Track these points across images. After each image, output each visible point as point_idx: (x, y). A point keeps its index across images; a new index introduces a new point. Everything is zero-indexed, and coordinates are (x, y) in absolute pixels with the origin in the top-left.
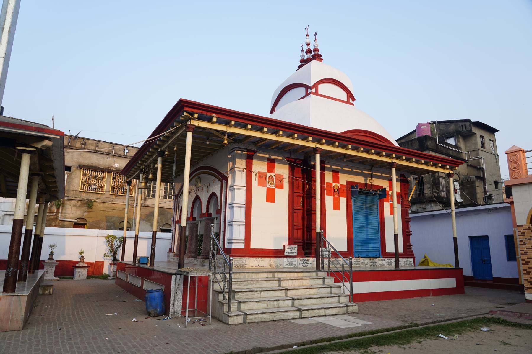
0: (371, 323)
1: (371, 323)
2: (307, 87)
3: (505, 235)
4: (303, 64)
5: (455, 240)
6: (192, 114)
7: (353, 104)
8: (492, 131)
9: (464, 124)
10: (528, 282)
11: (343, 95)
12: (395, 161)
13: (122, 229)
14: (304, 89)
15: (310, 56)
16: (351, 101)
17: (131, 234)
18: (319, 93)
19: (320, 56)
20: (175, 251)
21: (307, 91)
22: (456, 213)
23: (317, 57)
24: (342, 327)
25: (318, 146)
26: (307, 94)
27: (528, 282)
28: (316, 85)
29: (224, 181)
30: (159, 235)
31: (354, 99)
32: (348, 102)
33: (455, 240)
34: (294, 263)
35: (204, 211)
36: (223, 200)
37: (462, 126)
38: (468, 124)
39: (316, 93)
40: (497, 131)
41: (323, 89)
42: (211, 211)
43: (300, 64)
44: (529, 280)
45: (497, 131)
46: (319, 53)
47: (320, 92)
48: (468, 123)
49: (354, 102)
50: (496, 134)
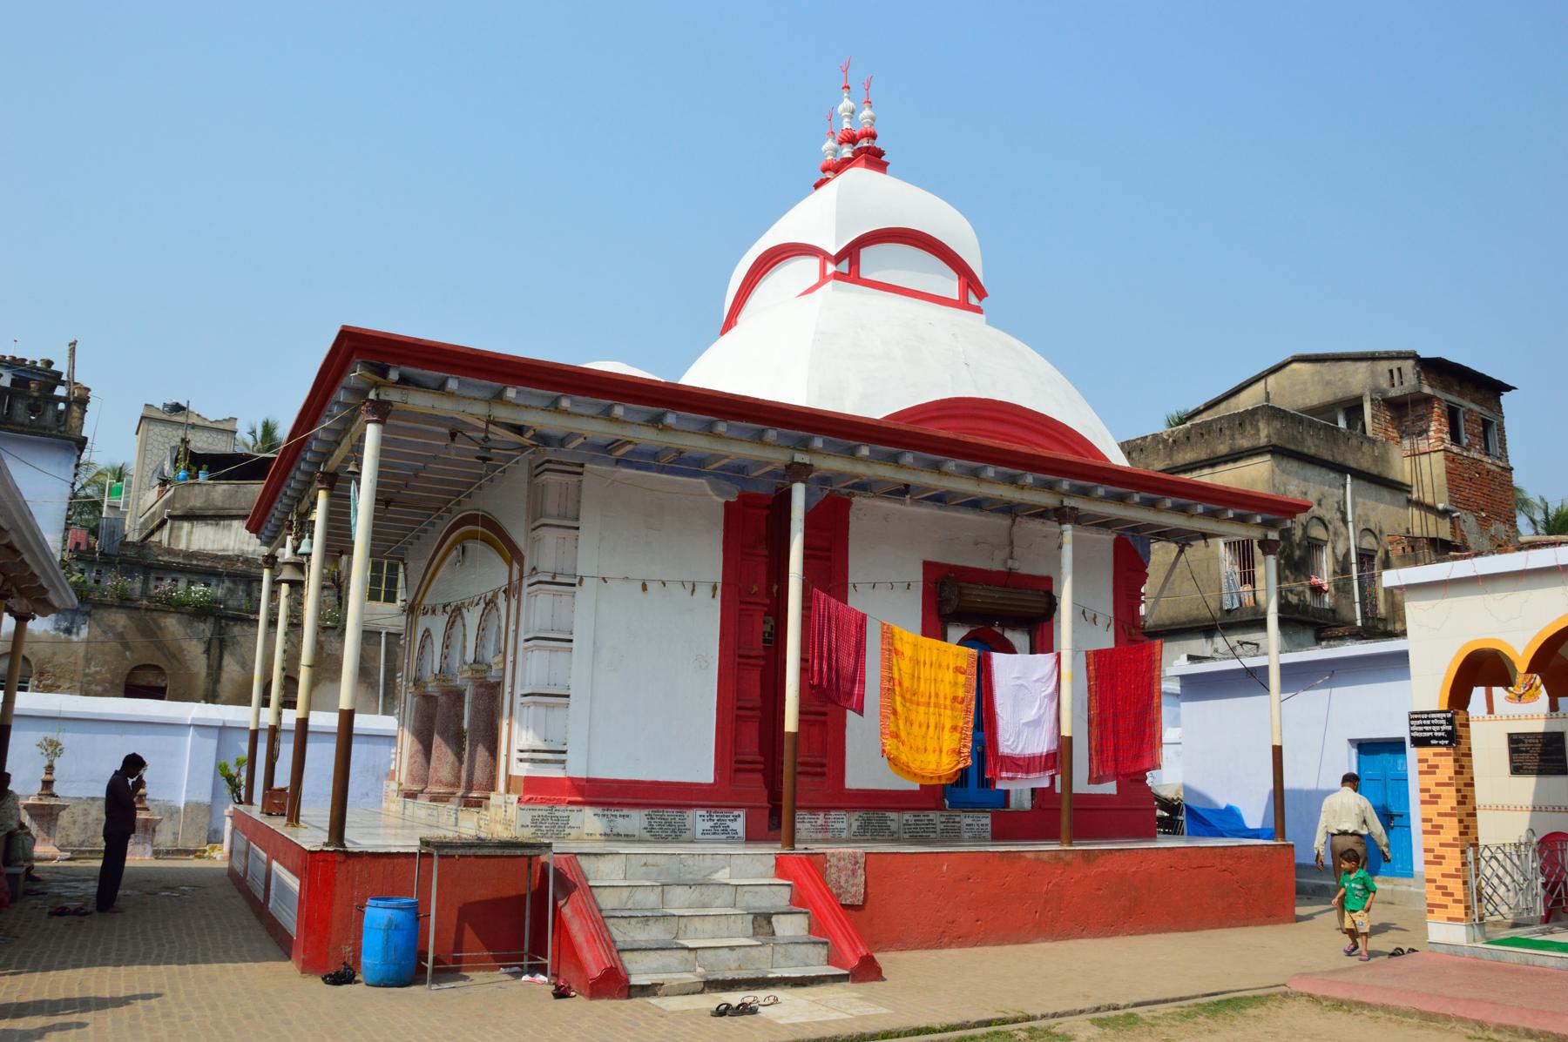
0: (885, 1011)
1: (885, 1011)
4: (829, 175)
5: (1277, 752)
6: (383, 373)
7: (978, 310)
8: (1491, 389)
9: (1395, 364)
10: (1438, 888)
12: (1068, 502)
13: (248, 703)
14: (813, 263)
15: (847, 151)
16: (973, 300)
17: (290, 718)
18: (863, 275)
19: (882, 153)
20: (403, 779)
22: (1285, 668)
24: (780, 1022)
25: (800, 458)
26: (824, 279)
27: (1438, 888)
28: (851, 252)
29: (516, 567)
30: (362, 722)
31: (981, 294)
32: (962, 304)
33: (1277, 752)
34: (732, 825)
35: (470, 657)
36: (512, 627)
37: (1391, 371)
38: (1408, 365)
39: (853, 276)
40: (1509, 388)
41: (874, 262)
42: (490, 655)
44: (1442, 882)
45: (1509, 388)
46: (878, 144)
47: (865, 274)
48: (1411, 363)
49: (983, 304)
50: (1505, 398)
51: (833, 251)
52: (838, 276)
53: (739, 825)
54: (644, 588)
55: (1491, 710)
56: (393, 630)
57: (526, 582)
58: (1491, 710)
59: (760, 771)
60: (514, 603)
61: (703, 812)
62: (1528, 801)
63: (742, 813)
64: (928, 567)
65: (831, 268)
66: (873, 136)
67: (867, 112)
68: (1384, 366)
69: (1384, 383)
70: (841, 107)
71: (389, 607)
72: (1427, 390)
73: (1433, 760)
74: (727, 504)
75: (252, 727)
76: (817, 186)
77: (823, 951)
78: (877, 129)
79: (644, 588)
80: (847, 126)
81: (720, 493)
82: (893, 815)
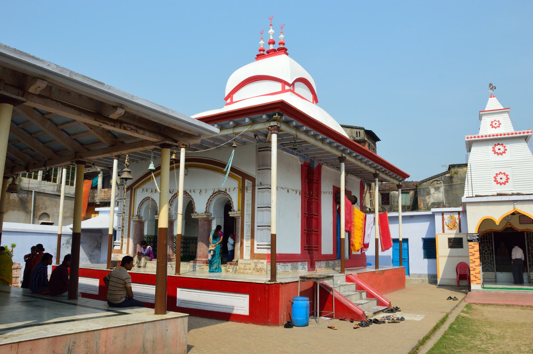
2: (284, 83)
3: (422, 238)
9: (358, 131)
11: (310, 96)
15: (272, 47)
19: (286, 50)
21: (283, 88)
23: (283, 50)
28: (293, 84)
38: (362, 132)
39: (293, 91)
40: (379, 140)
43: (259, 53)
45: (379, 140)
46: (285, 46)
47: (296, 90)
51: (291, 83)
52: (290, 90)
53: (306, 267)
54: (288, 191)
55: (444, 232)
56: (37, 190)
57: (257, 188)
58: (444, 232)
59: (269, 248)
60: (248, 195)
61: (300, 263)
62: (447, 254)
63: (306, 263)
64: (334, 187)
65: (287, 88)
66: (284, 44)
67: (282, 36)
68: (355, 130)
69: (355, 135)
70: (270, 31)
71: (35, 180)
72: (366, 139)
73: (473, 245)
74: (302, 165)
75: (59, 233)
76: (259, 57)
77: (375, 302)
78: (284, 42)
79: (288, 191)
80: (271, 38)
81: (300, 161)
82: (330, 262)
